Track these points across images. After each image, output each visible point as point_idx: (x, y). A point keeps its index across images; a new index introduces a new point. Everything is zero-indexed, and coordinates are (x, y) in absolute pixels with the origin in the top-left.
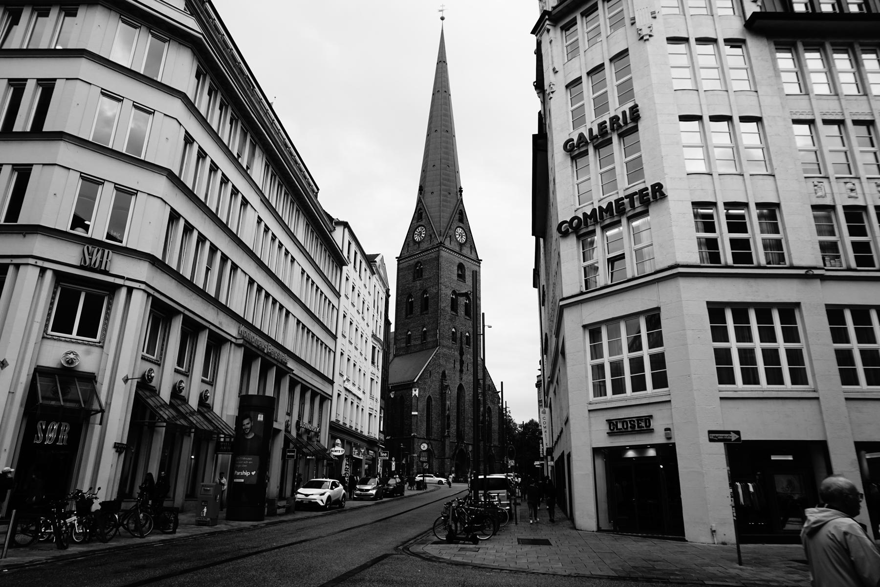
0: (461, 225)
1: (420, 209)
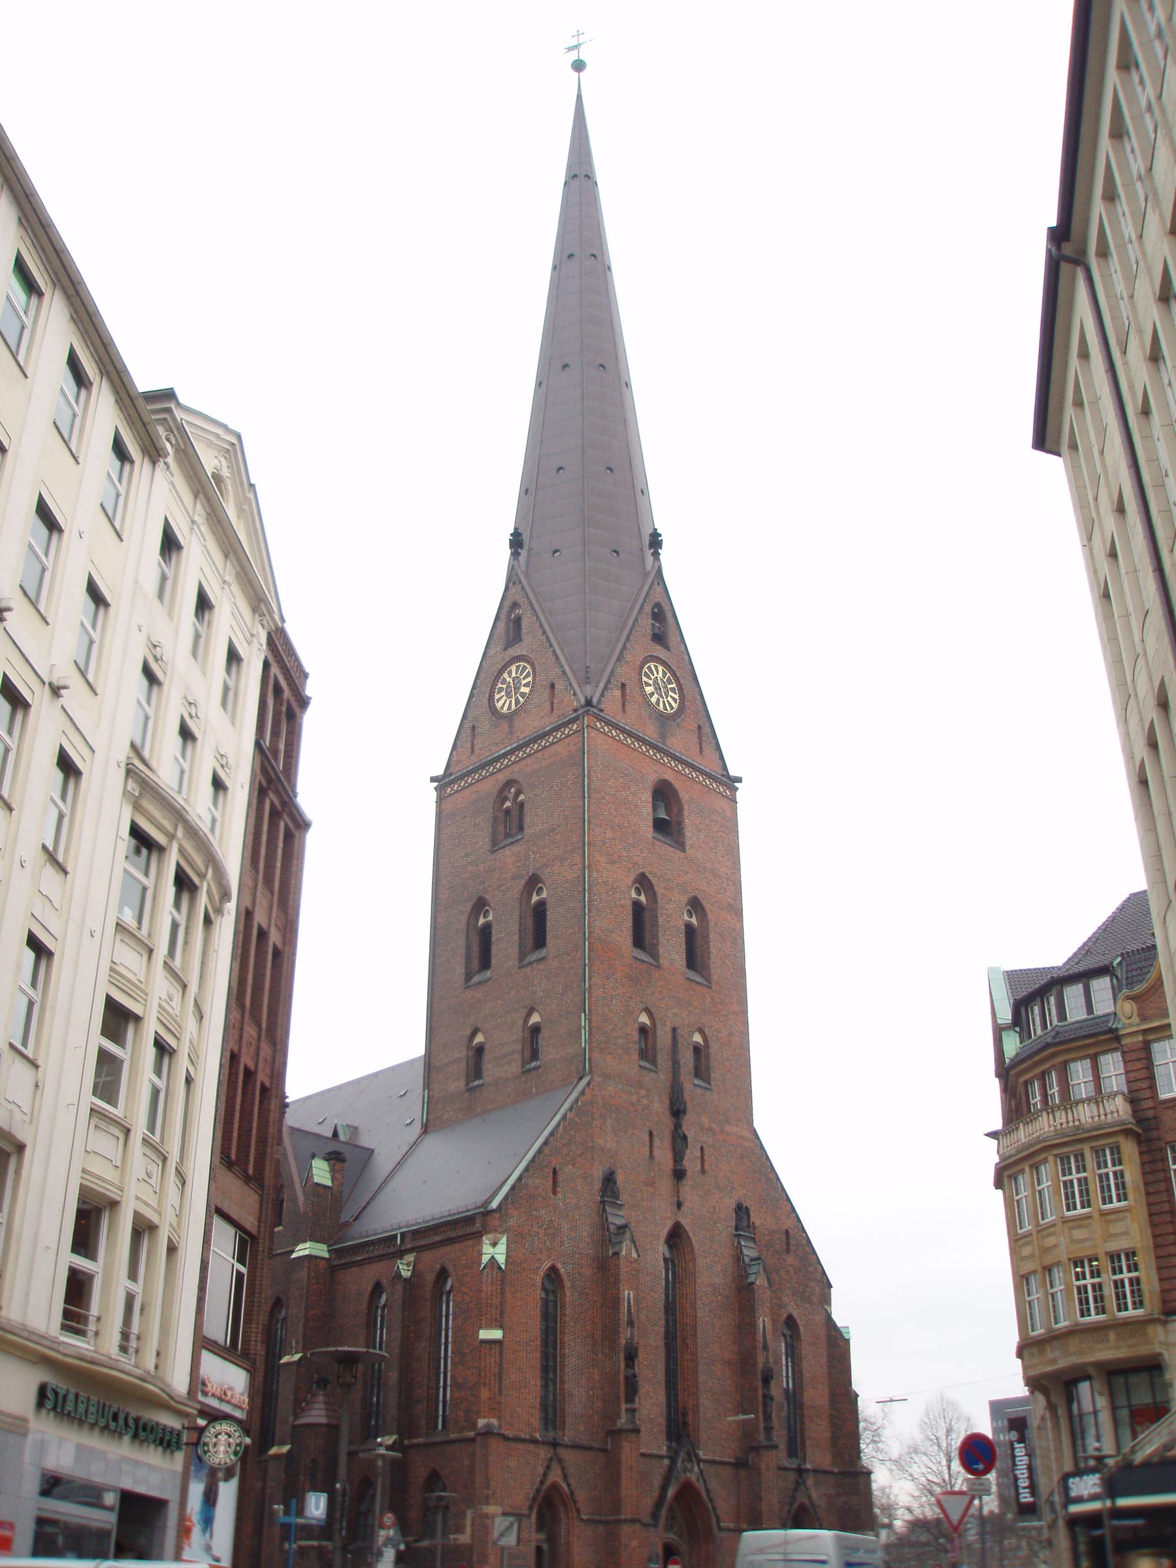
0: (660, 652)
1: (515, 605)
